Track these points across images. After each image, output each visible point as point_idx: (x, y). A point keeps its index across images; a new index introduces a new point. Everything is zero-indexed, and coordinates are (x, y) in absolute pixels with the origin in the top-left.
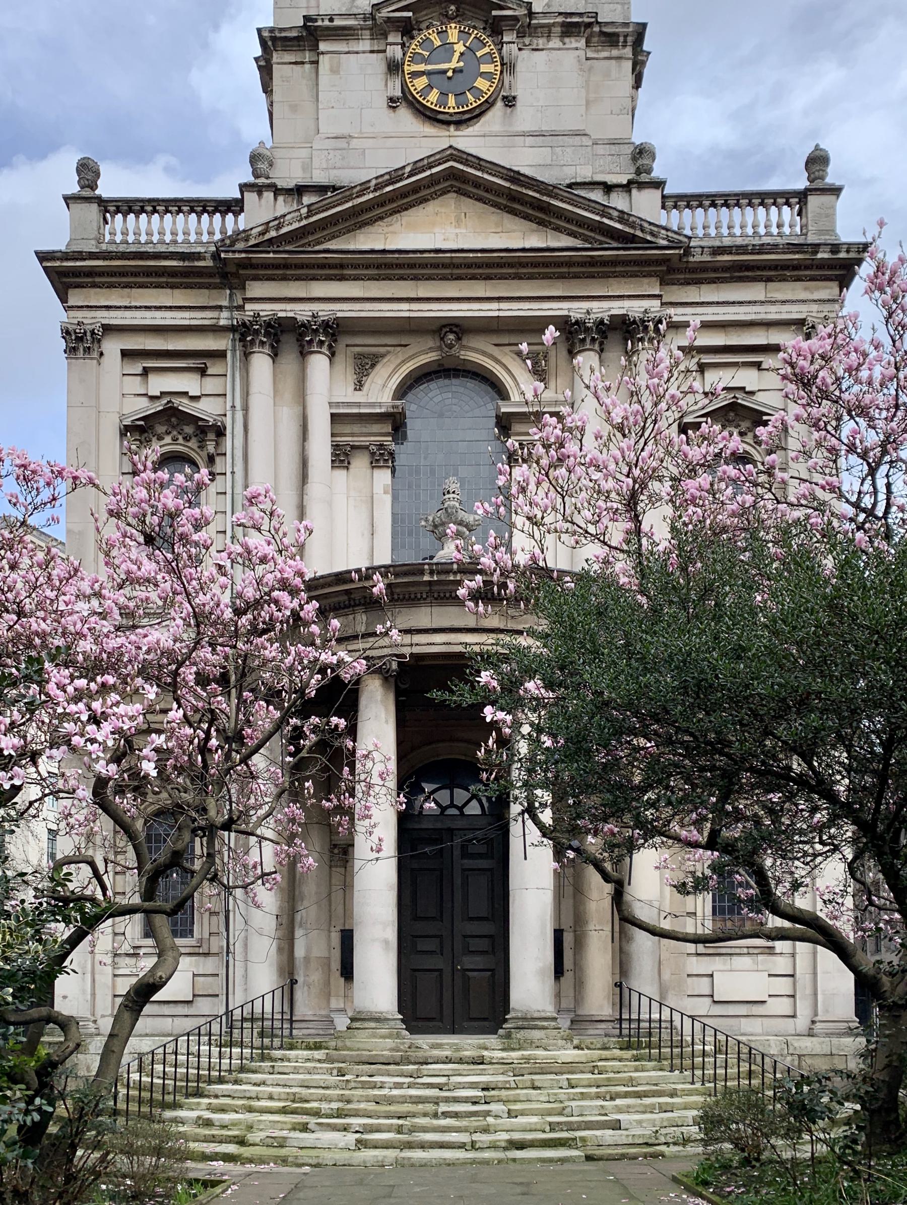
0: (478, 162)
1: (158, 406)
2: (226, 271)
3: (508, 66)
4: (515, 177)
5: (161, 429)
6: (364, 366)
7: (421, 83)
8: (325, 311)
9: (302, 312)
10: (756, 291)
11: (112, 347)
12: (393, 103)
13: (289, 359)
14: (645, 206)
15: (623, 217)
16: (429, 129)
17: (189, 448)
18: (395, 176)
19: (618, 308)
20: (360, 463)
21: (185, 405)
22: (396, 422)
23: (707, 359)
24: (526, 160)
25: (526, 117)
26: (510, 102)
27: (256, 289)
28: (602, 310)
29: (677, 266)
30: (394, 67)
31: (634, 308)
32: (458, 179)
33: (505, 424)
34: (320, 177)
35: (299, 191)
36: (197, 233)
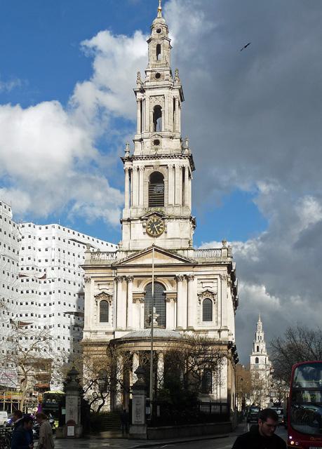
0: (159, 248)
1: (101, 292)
2: (113, 267)
3: (166, 226)
4: (165, 250)
5: (101, 295)
6: (139, 283)
7: (150, 229)
8: (132, 275)
9: (127, 275)
10: (211, 269)
11: (93, 280)
12: (144, 233)
13: (125, 282)
14: (190, 254)
15: (185, 258)
16: (151, 238)
17: (107, 299)
18: (144, 250)
19: (185, 273)
20: (138, 302)
21: (106, 291)
22: (145, 294)
23: (203, 281)
24: (168, 245)
25: (169, 235)
26: (166, 232)
27: (119, 270)
28: (182, 274)
29: (195, 265)
30: (144, 227)
31: (188, 274)
32: (158, 250)
33: (165, 294)
34: (131, 249)
35: (127, 252)
36: (109, 260)
